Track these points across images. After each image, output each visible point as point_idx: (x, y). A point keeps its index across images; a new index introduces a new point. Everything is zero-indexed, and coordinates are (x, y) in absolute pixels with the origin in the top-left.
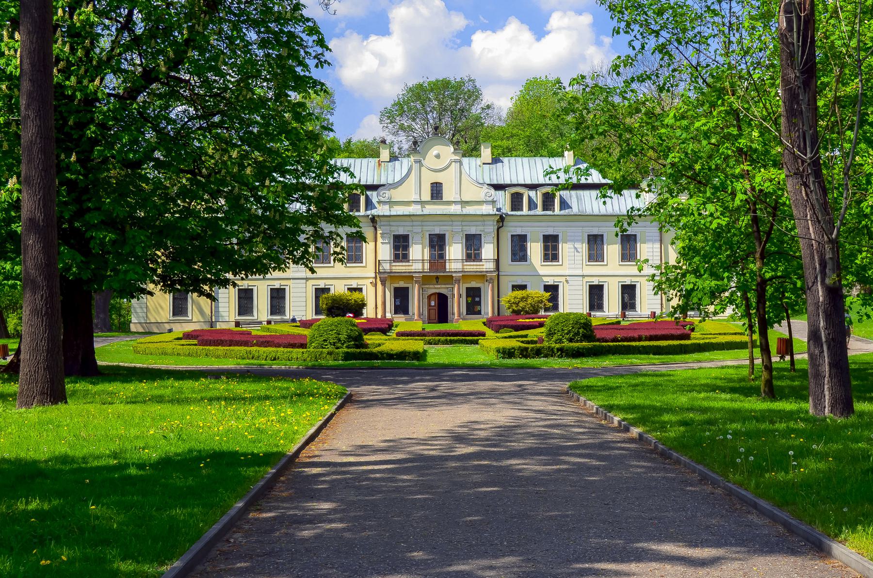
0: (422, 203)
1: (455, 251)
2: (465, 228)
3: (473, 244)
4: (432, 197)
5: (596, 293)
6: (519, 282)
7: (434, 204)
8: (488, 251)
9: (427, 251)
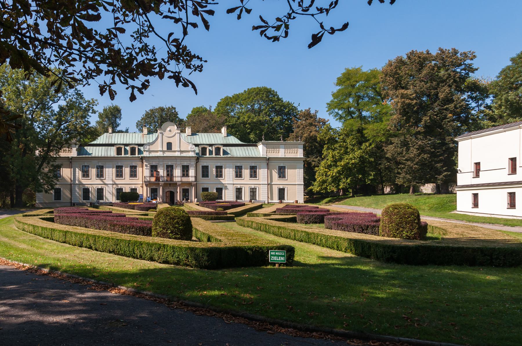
0: (163, 152)
1: (177, 172)
3: (185, 170)
4: (167, 149)
5: (239, 191)
6: (205, 186)
8: (192, 172)
9: (165, 172)
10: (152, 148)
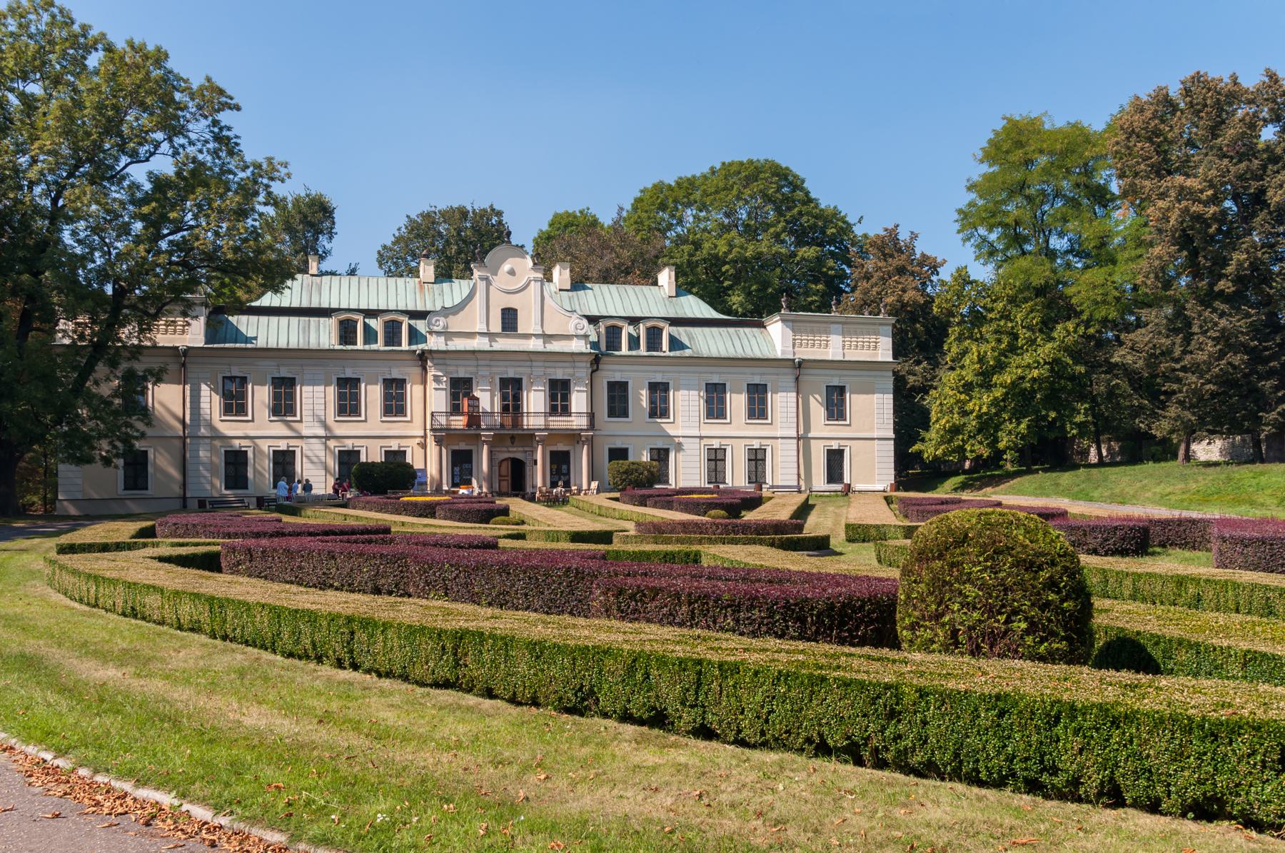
0: (491, 336)
1: (535, 401)
2: (549, 370)
3: (559, 393)
4: (504, 329)
5: (716, 459)
7: (507, 336)
8: (579, 401)
10: (456, 323)
